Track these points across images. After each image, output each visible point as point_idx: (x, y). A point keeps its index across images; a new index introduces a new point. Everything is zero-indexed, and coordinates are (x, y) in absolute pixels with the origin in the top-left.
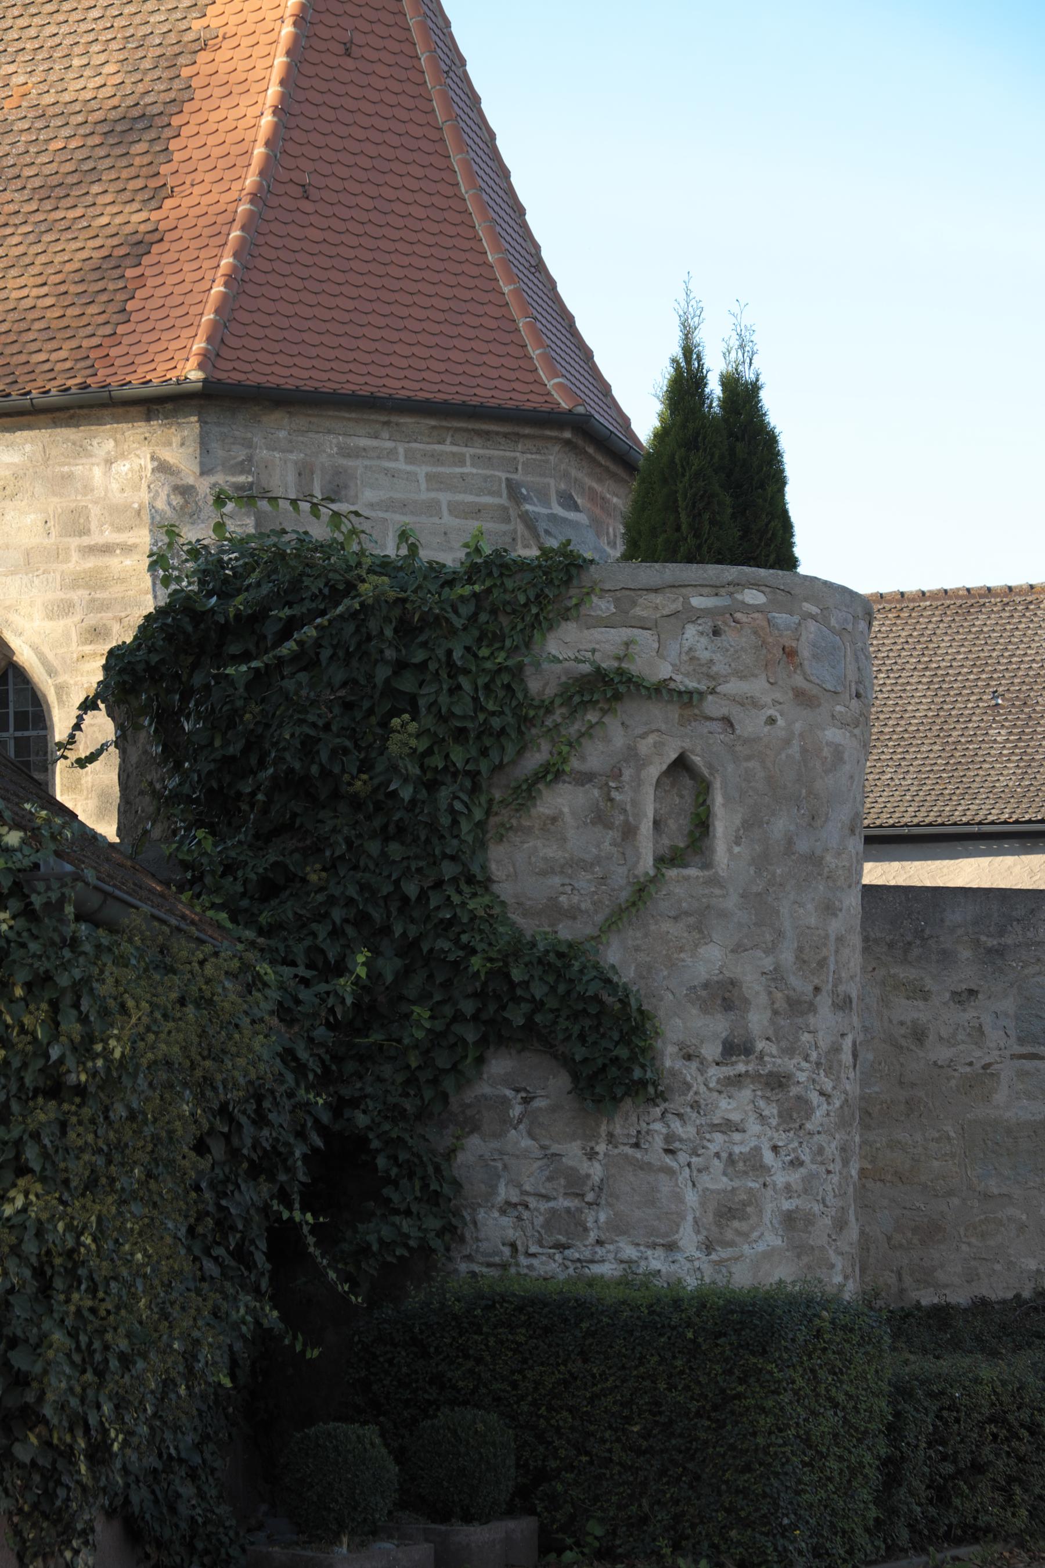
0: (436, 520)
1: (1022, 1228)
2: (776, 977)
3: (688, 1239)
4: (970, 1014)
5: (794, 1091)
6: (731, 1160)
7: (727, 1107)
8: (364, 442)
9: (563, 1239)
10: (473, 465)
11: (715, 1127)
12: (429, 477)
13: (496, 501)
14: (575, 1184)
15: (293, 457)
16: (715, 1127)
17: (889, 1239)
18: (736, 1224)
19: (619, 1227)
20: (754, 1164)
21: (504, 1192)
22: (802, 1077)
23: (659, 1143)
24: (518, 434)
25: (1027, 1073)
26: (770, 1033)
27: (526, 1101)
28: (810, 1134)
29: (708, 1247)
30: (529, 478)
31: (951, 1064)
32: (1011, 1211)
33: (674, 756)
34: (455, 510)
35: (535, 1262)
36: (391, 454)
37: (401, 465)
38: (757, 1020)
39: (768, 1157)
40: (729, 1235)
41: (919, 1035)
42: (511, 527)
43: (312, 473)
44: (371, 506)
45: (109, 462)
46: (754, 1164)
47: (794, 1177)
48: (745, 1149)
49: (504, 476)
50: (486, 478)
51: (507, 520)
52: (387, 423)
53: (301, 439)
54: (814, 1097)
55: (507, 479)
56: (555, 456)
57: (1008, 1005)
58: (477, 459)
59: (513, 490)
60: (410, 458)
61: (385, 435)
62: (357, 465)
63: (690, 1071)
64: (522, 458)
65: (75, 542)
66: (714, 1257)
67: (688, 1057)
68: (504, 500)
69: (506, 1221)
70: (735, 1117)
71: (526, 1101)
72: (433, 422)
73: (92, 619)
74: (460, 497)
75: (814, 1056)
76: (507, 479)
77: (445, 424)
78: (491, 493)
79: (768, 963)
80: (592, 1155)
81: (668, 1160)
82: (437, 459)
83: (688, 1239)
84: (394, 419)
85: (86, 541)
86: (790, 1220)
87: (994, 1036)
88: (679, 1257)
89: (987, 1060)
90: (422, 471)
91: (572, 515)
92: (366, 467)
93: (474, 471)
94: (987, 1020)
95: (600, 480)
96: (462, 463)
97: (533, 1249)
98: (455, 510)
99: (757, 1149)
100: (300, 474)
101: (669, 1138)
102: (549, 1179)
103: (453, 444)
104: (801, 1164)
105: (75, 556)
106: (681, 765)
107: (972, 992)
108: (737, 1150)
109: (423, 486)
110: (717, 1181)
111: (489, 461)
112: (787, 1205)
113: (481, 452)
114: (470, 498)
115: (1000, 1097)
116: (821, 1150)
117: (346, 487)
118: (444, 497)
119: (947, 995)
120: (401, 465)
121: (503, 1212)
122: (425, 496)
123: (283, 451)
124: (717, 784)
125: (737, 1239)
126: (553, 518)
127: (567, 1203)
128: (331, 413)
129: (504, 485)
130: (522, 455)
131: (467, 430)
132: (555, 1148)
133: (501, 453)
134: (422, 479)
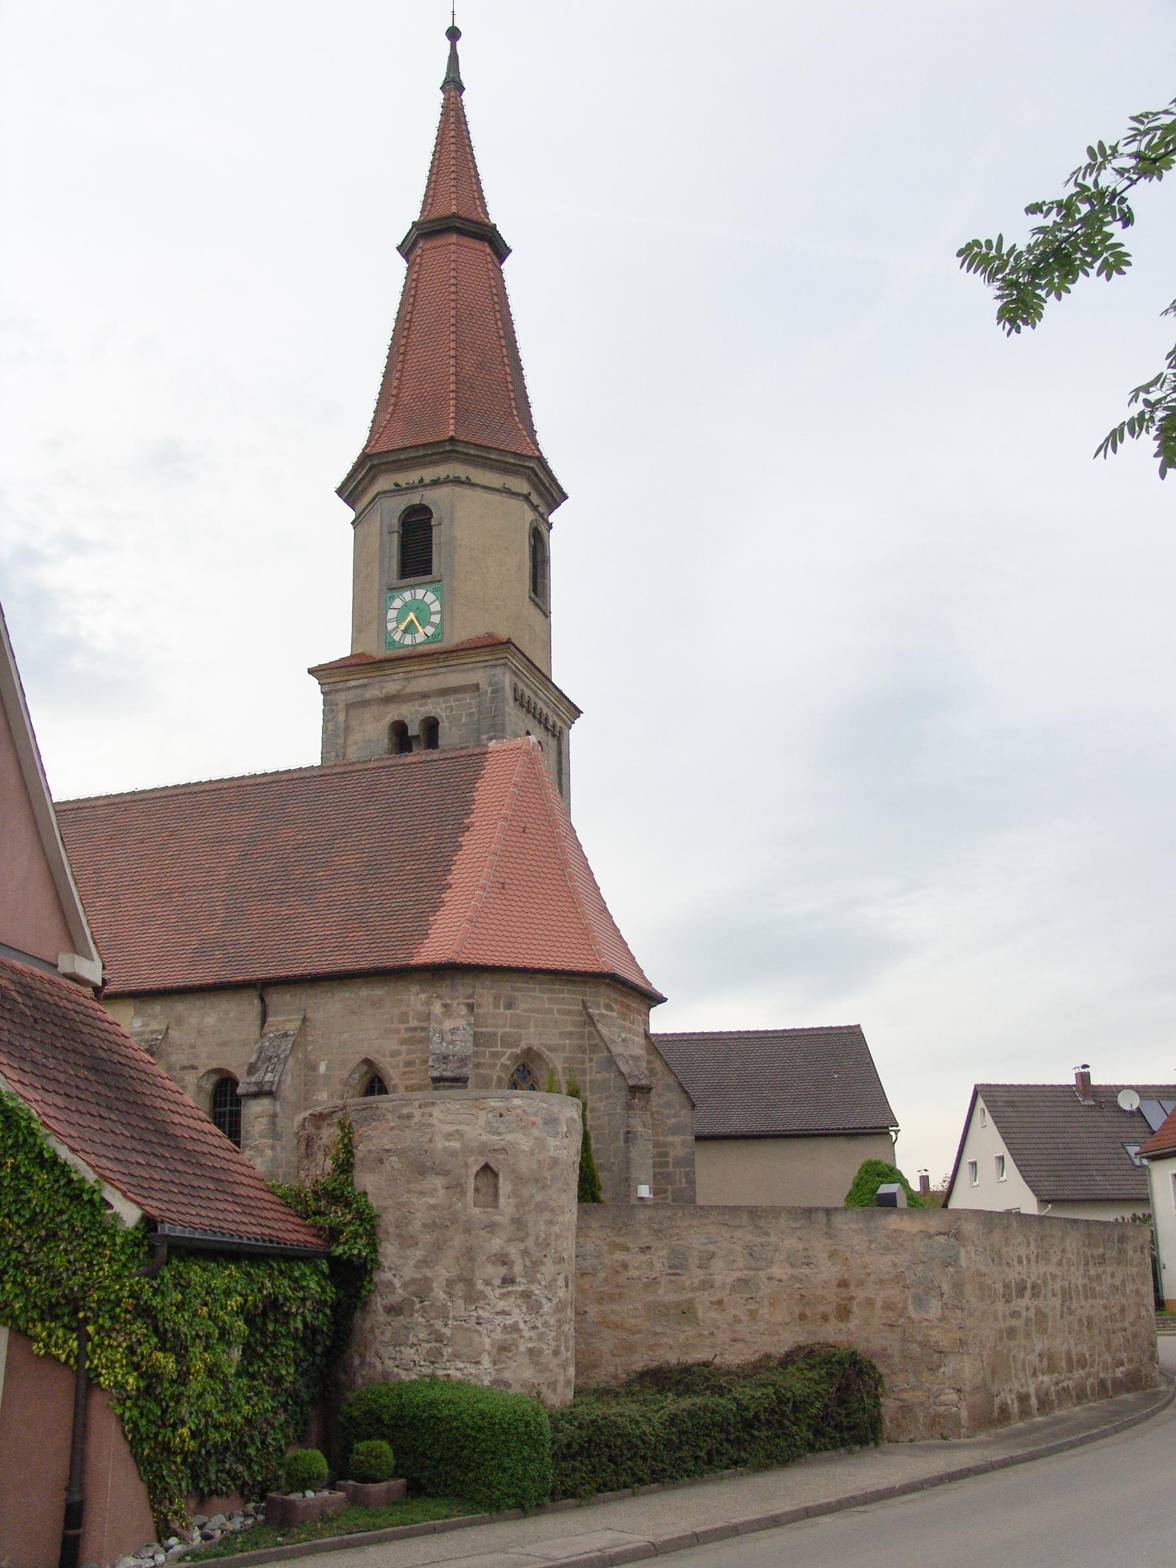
1: (671, 1347)
2: (525, 1253)
3: (486, 1362)
4: (648, 1257)
5: (534, 1298)
6: (505, 1327)
7: (502, 1305)
8: (523, 985)
9: (433, 1359)
11: (498, 1313)
12: (549, 998)
14: (439, 1338)
16: (498, 1313)
17: (611, 1351)
18: (507, 1353)
19: (456, 1356)
20: (515, 1328)
21: (412, 1340)
22: (537, 1292)
23: (474, 1320)
25: (673, 1281)
26: (523, 1274)
27: (421, 1302)
28: (542, 1316)
29: (495, 1363)
31: (639, 1278)
32: (665, 1340)
33: (482, 1164)
35: (423, 1369)
36: (533, 990)
38: (518, 1268)
39: (522, 1325)
40: (503, 1358)
41: (625, 1266)
44: (525, 1011)
45: (417, 994)
46: (515, 1328)
47: (533, 1334)
48: (511, 1322)
49: (580, 998)
50: (573, 999)
51: (582, 1016)
54: (544, 1301)
56: (603, 990)
57: (664, 1253)
58: (569, 991)
59: (584, 1004)
63: (488, 1290)
64: (588, 991)
65: (403, 1026)
66: (497, 1367)
67: (487, 1284)
68: (581, 1008)
69: (412, 1351)
70: (507, 1309)
71: (421, 1302)
73: (409, 1058)
74: (562, 1007)
75: (543, 1283)
79: (522, 1246)
80: (446, 1325)
81: (478, 1327)
82: (551, 990)
83: (486, 1362)
84: (534, 976)
85: (407, 1026)
86: (530, 1350)
87: (658, 1266)
88: (481, 1367)
89: (655, 1276)
90: (546, 996)
91: (609, 1013)
94: (655, 1259)
95: (625, 997)
97: (422, 1363)
98: (559, 1011)
99: (516, 1323)
101: (478, 1318)
102: (429, 1334)
104: (537, 1328)
105: (403, 1031)
106: (486, 1168)
107: (649, 1248)
108: (508, 1322)
110: (498, 1335)
112: (530, 1345)
114: (567, 1007)
115: (660, 1292)
116: (546, 1322)
118: (555, 1007)
119: (637, 1249)
121: (411, 1347)
122: (547, 1006)
124: (501, 1175)
125: (507, 1360)
126: (601, 1015)
127: (436, 1345)
132: (431, 1322)
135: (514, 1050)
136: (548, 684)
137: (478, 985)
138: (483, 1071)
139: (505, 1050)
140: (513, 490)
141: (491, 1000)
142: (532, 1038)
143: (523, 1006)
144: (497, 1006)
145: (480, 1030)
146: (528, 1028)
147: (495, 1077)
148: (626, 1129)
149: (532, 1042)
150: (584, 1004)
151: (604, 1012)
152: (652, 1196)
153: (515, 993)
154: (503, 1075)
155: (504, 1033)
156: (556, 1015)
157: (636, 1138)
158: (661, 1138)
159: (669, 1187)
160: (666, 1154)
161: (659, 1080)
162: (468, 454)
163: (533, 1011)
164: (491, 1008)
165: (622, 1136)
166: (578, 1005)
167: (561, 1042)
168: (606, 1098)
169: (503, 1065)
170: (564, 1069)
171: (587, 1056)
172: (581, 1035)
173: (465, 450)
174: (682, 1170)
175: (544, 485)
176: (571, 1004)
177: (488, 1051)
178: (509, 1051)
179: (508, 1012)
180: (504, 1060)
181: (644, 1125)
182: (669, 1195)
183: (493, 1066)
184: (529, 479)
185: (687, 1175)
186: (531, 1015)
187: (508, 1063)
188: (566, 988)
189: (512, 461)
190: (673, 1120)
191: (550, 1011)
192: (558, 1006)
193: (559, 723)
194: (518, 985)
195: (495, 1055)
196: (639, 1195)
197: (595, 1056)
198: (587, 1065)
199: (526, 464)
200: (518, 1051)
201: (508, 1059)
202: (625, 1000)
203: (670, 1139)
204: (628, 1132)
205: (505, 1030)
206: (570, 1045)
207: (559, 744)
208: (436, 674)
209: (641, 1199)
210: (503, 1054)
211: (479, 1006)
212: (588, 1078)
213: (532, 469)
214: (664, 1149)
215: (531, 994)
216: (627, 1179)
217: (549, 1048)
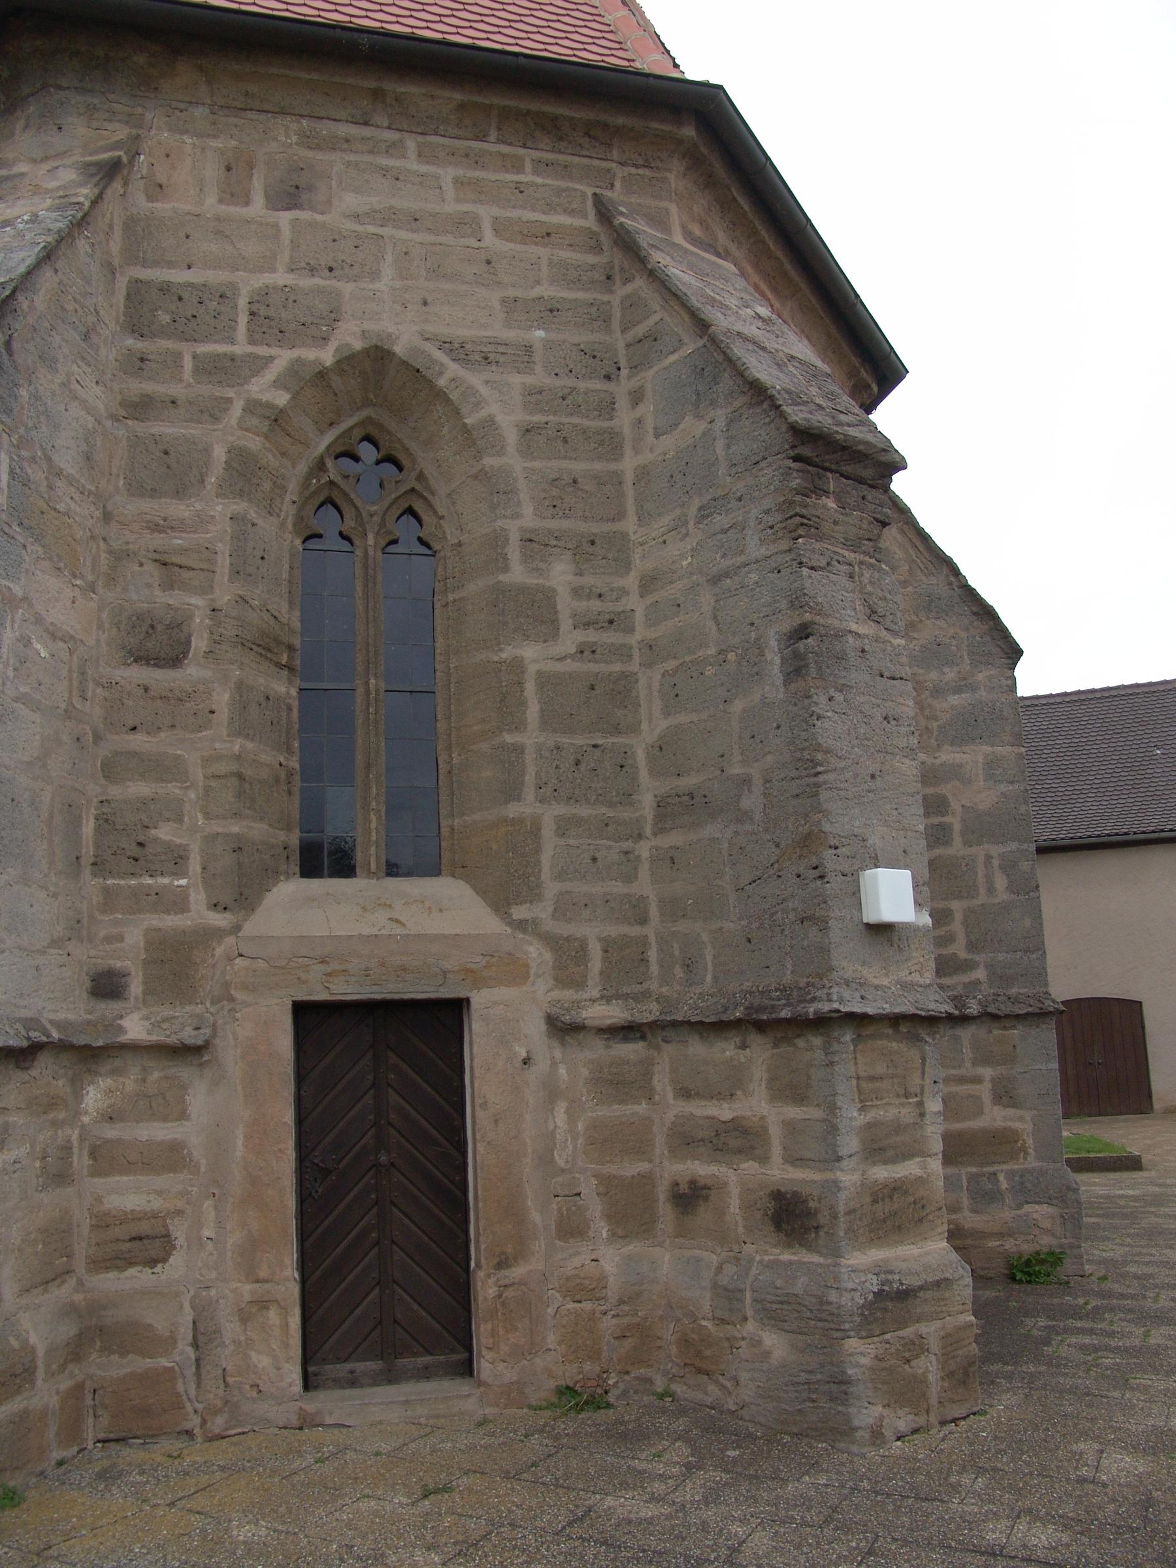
8: (344, 129)
10: (536, 172)
12: (456, 181)
13: (578, 222)
24: (605, 126)
30: (634, 199)
36: (392, 149)
37: (413, 165)
42: (602, 259)
43: (251, 166)
44: (356, 217)
50: (559, 192)
51: (597, 249)
52: (377, 95)
53: (234, 120)
55: (595, 194)
58: (542, 167)
59: (604, 213)
62: (335, 161)
64: (620, 172)
68: (590, 222)
72: (458, 96)
76: (595, 194)
90: (448, 174)
92: (348, 164)
93: (539, 180)
96: (520, 169)
100: (229, 169)
103: (500, 141)
109: (450, 193)
117: (311, 188)
118: (486, 213)
122: (451, 207)
123: (200, 135)
128: (274, 70)
129: (590, 203)
133: (585, 161)
135: (310, 354)
137: (154, 116)
138: (165, 429)
139: (263, 351)
141: (212, 171)
143: (350, 201)
144: (236, 194)
146: (375, 275)
147: (220, 453)
148: (787, 624)
150: (604, 213)
152: (926, 920)
154: (254, 443)
155: (265, 293)
156: (489, 238)
163: (390, 217)
164: (211, 200)
165: (774, 658)
166: (586, 217)
167: (510, 335)
168: (704, 514)
169: (252, 407)
170: (527, 430)
171: (622, 388)
172: (601, 317)
174: (996, 850)
176: (551, 208)
177: (188, 354)
178: (283, 357)
179: (285, 218)
181: (872, 614)
183: (213, 411)
186: (386, 231)
187: (282, 399)
188: (529, 155)
190: (955, 700)
191: (465, 224)
192: (497, 212)
194: (325, 128)
196: (870, 917)
197: (649, 377)
198: (624, 419)
200: (327, 356)
201: (277, 384)
204: (803, 632)
205: (268, 279)
206: (548, 345)
209: (882, 930)
210: (259, 364)
211: (157, 190)
212: (628, 464)
216: (810, 841)
217: (458, 350)
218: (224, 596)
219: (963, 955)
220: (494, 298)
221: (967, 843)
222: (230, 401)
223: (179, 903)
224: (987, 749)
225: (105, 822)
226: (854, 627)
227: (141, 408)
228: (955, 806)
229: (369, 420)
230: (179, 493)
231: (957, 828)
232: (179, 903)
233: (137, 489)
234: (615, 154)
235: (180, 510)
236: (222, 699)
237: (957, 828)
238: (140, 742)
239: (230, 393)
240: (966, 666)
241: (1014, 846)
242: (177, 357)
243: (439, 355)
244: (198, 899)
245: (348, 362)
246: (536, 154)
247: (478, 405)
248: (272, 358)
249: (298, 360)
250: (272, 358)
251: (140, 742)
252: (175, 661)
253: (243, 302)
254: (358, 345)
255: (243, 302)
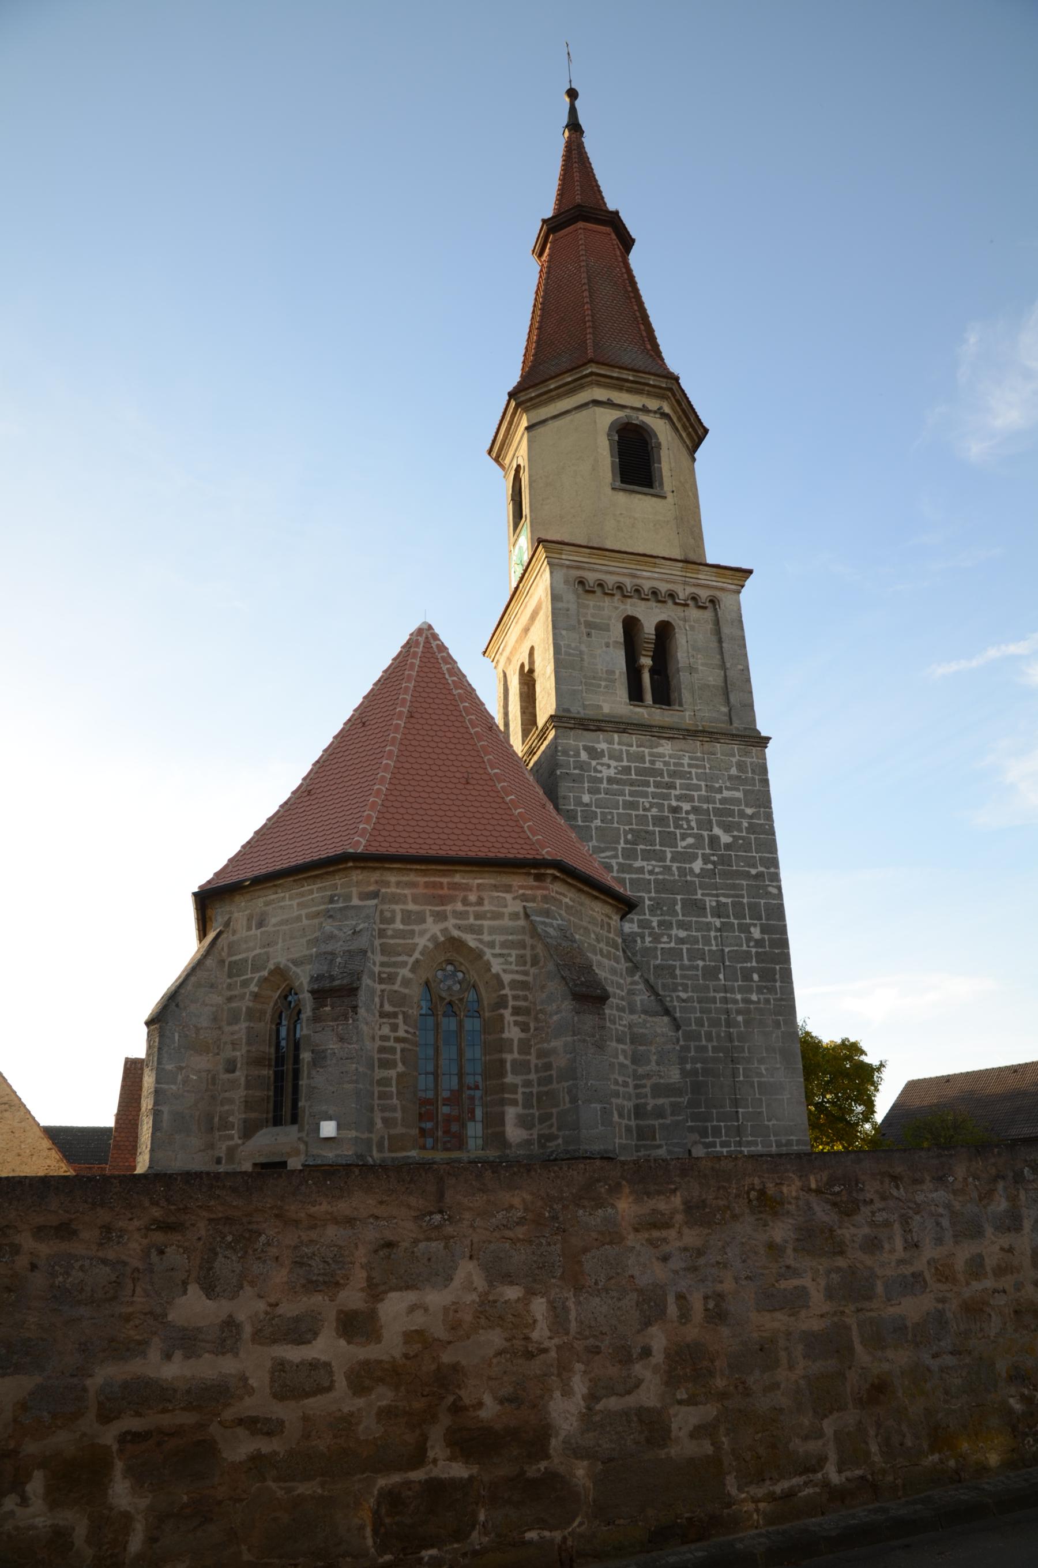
0: (300, 924)
12: (298, 904)
15: (246, 913)
34: (309, 917)
36: (284, 898)
44: (274, 925)
56: (356, 876)
58: (320, 889)
60: (291, 899)
61: (280, 891)
62: (269, 908)
64: (339, 882)
72: (291, 879)
74: (310, 910)
77: (296, 878)
78: (324, 903)
82: (302, 895)
84: (276, 883)
90: (295, 903)
95: (440, 876)
98: (309, 917)
103: (308, 885)
111: (324, 889)
113: (321, 885)
114: (314, 909)
117: (265, 919)
118: (303, 912)
120: (287, 903)
122: (296, 914)
130: (338, 880)
131: (305, 879)
134: (295, 906)
136: (657, 561)
138: (234, 1005)
139: (254, 975)
140: (615, 402)
141: (245, 923)
142: (280, 957)
144: (249, 928)
145: (234, 958)
146: (277, 943)
147: (244, 1009)
149: (279, 960)
151: (355, 901)
153: (267, 908)
155: (254, 957)
156: (305, 922)
157: (325, 1057)
158: (545, 1045)
159: (554, 1111)
160: (548, 1067)
161: (543, 967)
162: (531, 399)
167: (307, 953)
169: (251, 992)
173: (528, 396)
174: (566, 1084)
175: (627, 381)
178: (257, 975)
179: (259, 931)
180: (254, 988)
182: (554, 1120)
184: (599, 384)
185: (569, 1092)
187: (256, 989)
188: (315, 887)
189: (570, 379)
190: (555, 1018)
193: (704, 594)
195: (245, 984)
199: (584, 373)
202: (445, 880)
203: (554, 1044)
207: (716, 615)
208: (526, 606)
210: (252, 979)
211: (234, 932)
213: (592, 374)
214: (546, 1060)
215: (282, 904)
217: (296, 963)
218: (244, 1051)
219: (556, 1133)
220: (304, 941)
221: (558, 1083)
222: (246, 993)
223: (231, 1137)
224: (564, 1039)
225: (220, 1117)
226: (331, 1047)
227: (230, 999)
228: (554, 1066)
229: (288, 985)
230: (236, 1023)
231: (555, 1076)
232: (231, 1137)
233: (229, 1024)
234: (337, 877)
235: (236, 1028)
236: (243, 1080)
237: (555, 1076)
238: (227, 1095)
239: (246, 990)
240: (559, 1002)
241: (571, 1082)
242: (236, 982)
243: (291, 965)
244: (236, 1136)
245: (272, 973)
246: (317, 886)
247: (299, 979)
248: (254, 978)
249: (260, 977)
250: (254, 978)
251: (227, 1095)
252: (233, 1071)
253: (250, 962)
254: (272, 967)
255: (250, 962)
